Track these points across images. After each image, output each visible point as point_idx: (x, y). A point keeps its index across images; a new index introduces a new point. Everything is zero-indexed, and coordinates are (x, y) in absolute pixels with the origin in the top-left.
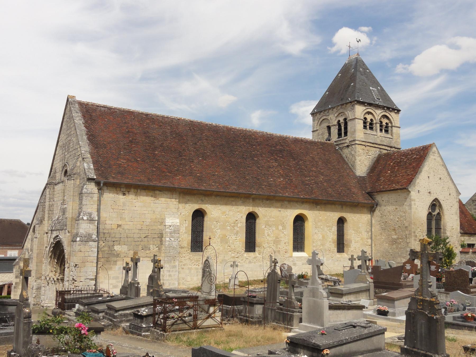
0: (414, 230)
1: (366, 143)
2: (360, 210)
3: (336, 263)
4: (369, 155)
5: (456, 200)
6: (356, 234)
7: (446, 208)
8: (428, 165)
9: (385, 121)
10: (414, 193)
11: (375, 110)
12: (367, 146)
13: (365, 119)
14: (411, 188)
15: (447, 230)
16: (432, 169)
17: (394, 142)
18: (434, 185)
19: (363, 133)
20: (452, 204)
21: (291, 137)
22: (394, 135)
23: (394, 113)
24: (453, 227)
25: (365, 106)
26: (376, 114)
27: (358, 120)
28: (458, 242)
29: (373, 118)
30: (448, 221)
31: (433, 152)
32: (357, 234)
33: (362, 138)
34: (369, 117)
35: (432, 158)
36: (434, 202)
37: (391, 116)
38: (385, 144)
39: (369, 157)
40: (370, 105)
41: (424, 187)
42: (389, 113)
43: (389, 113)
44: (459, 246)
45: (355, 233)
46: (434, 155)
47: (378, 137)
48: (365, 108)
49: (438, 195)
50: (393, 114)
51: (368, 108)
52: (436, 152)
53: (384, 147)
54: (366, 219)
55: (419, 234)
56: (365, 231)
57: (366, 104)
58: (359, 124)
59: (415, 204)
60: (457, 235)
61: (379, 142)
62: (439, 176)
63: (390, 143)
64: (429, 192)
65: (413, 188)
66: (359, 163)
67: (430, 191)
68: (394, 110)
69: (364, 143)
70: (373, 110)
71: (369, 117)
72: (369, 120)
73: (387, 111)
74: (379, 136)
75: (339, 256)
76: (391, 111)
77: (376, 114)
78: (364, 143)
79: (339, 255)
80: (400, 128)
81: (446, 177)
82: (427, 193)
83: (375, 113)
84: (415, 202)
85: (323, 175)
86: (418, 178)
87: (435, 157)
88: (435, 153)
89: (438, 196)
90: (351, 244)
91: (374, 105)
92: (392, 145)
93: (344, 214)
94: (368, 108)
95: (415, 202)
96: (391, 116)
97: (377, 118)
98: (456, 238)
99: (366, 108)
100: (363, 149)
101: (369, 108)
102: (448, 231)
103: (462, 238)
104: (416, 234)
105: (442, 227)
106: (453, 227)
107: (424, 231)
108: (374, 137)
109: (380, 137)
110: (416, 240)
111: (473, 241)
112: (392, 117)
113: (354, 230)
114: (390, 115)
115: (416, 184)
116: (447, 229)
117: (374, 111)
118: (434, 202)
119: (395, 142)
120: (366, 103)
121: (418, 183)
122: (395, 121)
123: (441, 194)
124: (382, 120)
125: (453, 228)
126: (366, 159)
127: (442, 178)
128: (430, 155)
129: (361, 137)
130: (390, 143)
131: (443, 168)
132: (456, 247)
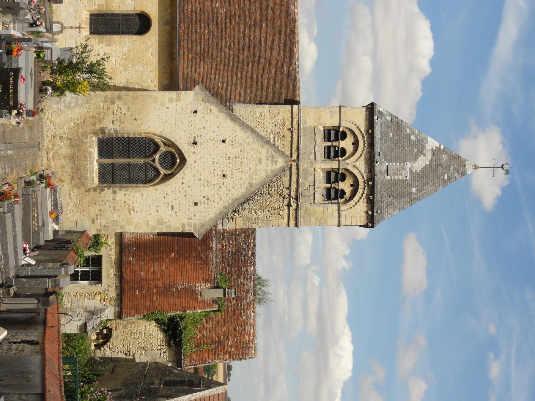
0: (124, 97)
1: (296, 131)
2: (164, 67)
3: (71, 9)
4: (274, 138)
5: (186, 221)
6: (122, 57)
7: (169, 192)
8: (247, 140)
9: (345, 186)
10: (192, 99)
11: (363, 156)
12: (292, 132)
13: (344, 136)
14: (201, 92)
15: (126, 192)
16: (241, 151)
17: (309, 206)
18: (210, 155)
19: (316, 124)
20: (178, 211)
21: (296, 11)
22: (322, 208)
23: (366, 209)
24: (133, 210)
25: (368, 132)
26: (357, 161)
27: (338, 112)
28: (105, 226)
29: (347, 154)
30: (145, 195)
31: (273, 156)
32: (123, 59)
33: (305, 123)
34: (347, 144)
35: (261, 153)
36: (178, 160)
37: (359, 201)
38: (301, 180)
39: (271, 136)
40: (371, 145)
41: (204, 128)
42: (364, 195)
43: (364, 195)
44: (97, 230)
45: (124, 54)
46: (267, 160)
47: (312, 162)
48: (363, 129)
49: (191, 165)
50: (363, 206)
51: (363, 138)
52: (275, 165)
53: (294, 179)
54: (150, 81)
55: (117, 111)
56: (127, 79)
57: (370, 131)
58: (331, 117)
59: (171, 100)
60: (117, 221)
61: (304, 165)
62: (228, 174)
63: (305, 196)
64: (197, 140)
65: (201, 97)
66: (258, 114)
67: (198, 143)
68: (371, 204)
69: (295, 125)
70: (363, 152)
71: (347, 144)
72: (343, 144)
73: (366, 188)
74: (315, 166)
75: (84, 16)
76: (368, 198)
77: (357, 161)
78: (295, 125)
79: (86, 18)
80: (339, 225)
81: (230, 193)
82: (193, 136)
83: (359, 158)
84: (174, 100)
85: (226, 14)
86: (220, 111)
87: (264, 161)
88: (272, 164)
89: (190, 167)
90: (104, 44)
91: (372, 153)
92: (301, 200)
93: (157, 29)
94: (365, 139)
95: (174, 100)
96: (359, 201)
97: (347, 161)
98: (111, 219)
99: (364, 133)
100: (284, 123)
101: (365, 141)
102: (125, 194)
103: (112, 241)
104: (117, 102)
105: (132, 185)
106: (133, 210)
107: (122, 125)
108: (311, 153)
109: (313, 170)
110: (106, 101)
111: (108, 276)
112: (356, 204)
113: (128, 51)
114: (361, 198)
115: (208, 105)
116: (129, 192)
117: (361, 155)
118: (178, 160)
119: (307, 209)
120: (373, 131)
121: (211, 110)
122: (349, 211)
123: (194, 176)
124: (349, 181)
125: (132, 212)
126: (267, 132)
127: (225, 180)
128: (268, 147)
129: (308, 121)
130: (305, 196)
131: (245, 186)
132: (95, 220)
